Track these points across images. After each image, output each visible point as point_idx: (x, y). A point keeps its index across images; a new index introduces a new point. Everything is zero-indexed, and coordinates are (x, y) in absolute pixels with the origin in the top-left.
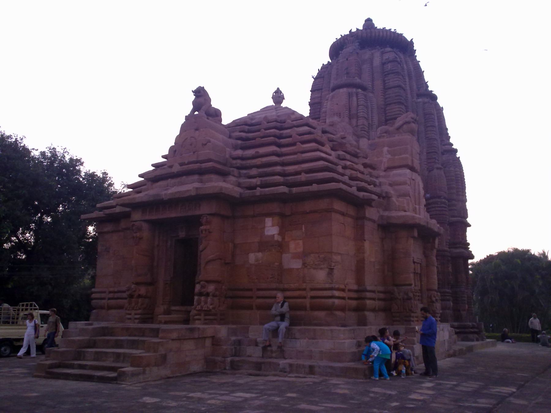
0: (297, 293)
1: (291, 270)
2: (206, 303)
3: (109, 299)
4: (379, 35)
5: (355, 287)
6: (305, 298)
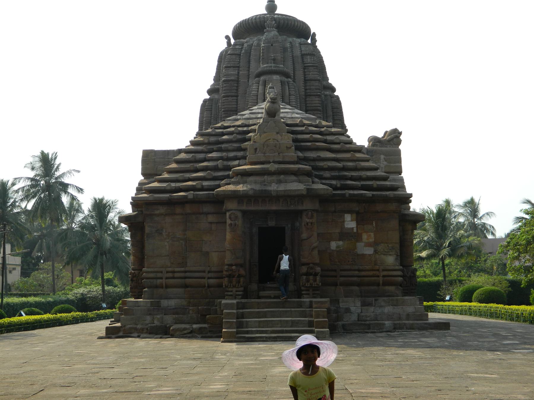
0: (371, 273)
1: (363, 255)
2: (315, 281)
3: (167, 278)
4: (294, 25)
6: (378, 276)
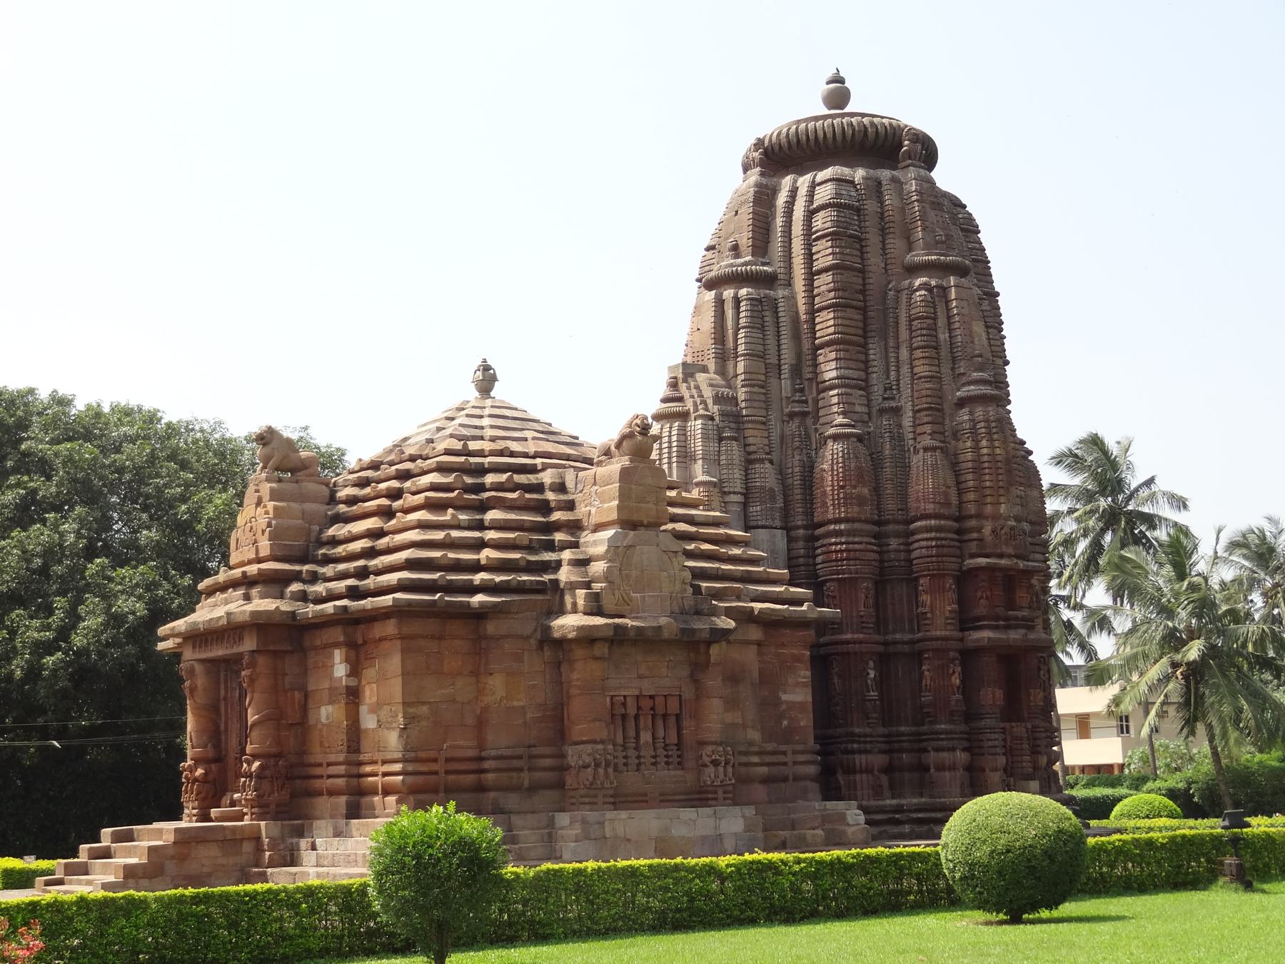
5: (471, 753)
